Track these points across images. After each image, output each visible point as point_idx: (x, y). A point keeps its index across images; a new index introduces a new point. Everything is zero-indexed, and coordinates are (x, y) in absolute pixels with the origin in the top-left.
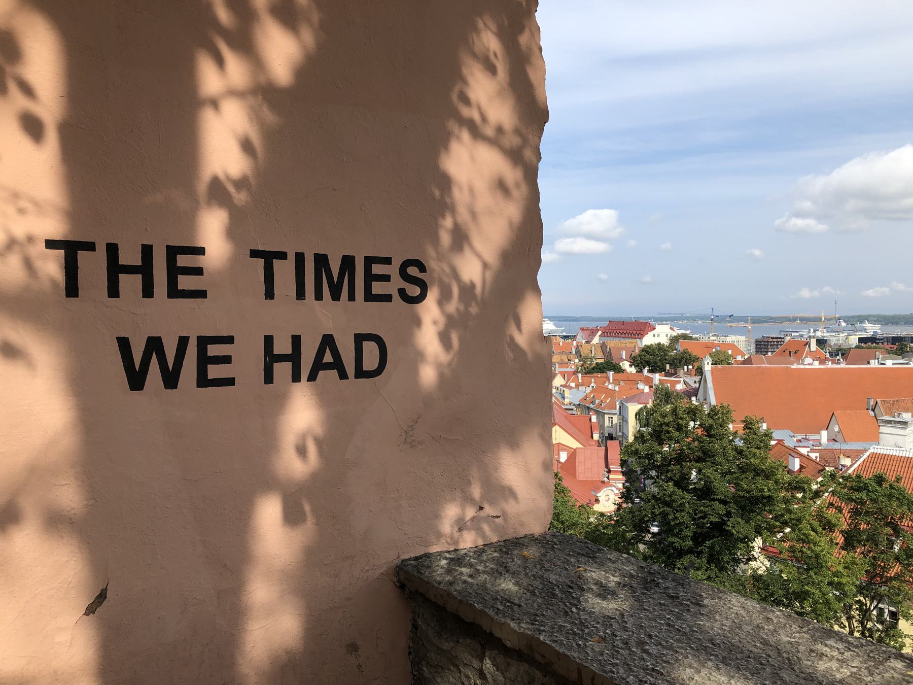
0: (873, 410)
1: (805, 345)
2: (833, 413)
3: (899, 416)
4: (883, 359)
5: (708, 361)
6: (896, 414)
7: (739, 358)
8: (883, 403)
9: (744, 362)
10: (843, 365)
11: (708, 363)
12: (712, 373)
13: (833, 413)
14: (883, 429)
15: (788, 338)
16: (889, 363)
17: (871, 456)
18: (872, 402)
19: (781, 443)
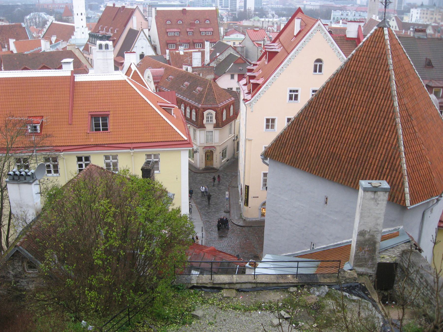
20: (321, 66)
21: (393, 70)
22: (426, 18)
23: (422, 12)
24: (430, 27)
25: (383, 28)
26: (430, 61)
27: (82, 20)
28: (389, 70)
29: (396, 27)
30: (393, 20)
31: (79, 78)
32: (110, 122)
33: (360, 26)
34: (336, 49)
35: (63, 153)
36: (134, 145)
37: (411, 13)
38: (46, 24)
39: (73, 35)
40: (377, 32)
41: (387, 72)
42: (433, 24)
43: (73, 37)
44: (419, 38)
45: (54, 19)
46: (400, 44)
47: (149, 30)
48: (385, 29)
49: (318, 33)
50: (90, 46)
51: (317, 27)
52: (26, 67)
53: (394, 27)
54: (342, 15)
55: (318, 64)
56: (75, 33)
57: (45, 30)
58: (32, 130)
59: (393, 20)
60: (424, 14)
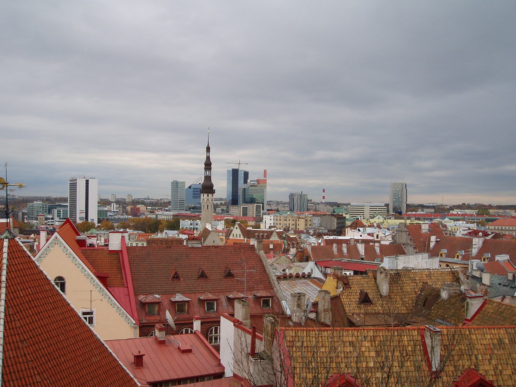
21: (6, 287)
22: (280, 224)
23: (276, 218)
24: (275, 234)
25: (4, 239)
26: (203, 271)
29: (240, 235)
30: (237, 228)
33: (123, 237)
34: (79, 264)
37: (264, 220)
42: (277, 231)
44: (193, 248)
46: (29, 257)
48: (5, 240)
49: (56, 246)
51: (54, 240)
53: (238, 236)
54: (191, 224)
59: (237, 228)
60: (277, 220)
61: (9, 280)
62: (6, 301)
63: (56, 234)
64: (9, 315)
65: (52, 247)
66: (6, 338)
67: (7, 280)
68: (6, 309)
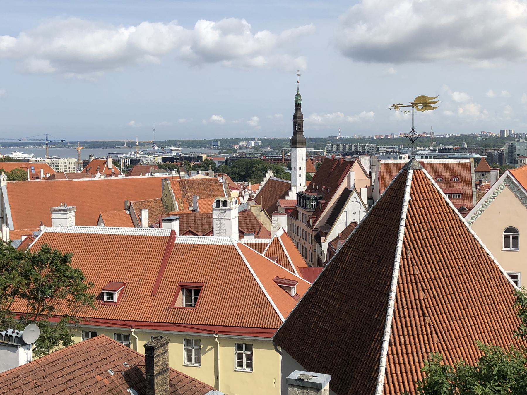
0: (129, 210)
1: (104, 164)
2: (100, 214)
3: (64, 206)
4: (155, 172)
5: (3, 178)
6: (62, 204)
7: (49, 175)
8: (135, 204)
9: (49, 178)
10: (121, 177)
11: (4, 179)
12: (7, 188)
13: (100, 214)
14: (54, 216)
15: (93, 158)
16: (157, 175)
17: (43, 235)
18: (128, 204)
19: (30, 237)
20: (516, 238)
27: (300, 176)
28: (399, 228)
31: (180, 240)
32: (201, 295)
35: (134, 330)
36: (221, 329)
38: (263, 181)
39: (288, 195)
40: (402, 176)
41: (397, 229)
43: (287, 198)
45: (272, 175)
46: (439, 192)
47: (373, 190)
50: (297, 209)
52: (191, 229)
55: (511, 234)
56: (290, 192)
57: (260, 188)
58: (109, 299)
61: (410, 218)
62: (404, 242)
63: (507, 173)
64: (407, 259)
65: (501, 189)
66: (401, 285)
67: (407, 217)
68: (404, 251)
